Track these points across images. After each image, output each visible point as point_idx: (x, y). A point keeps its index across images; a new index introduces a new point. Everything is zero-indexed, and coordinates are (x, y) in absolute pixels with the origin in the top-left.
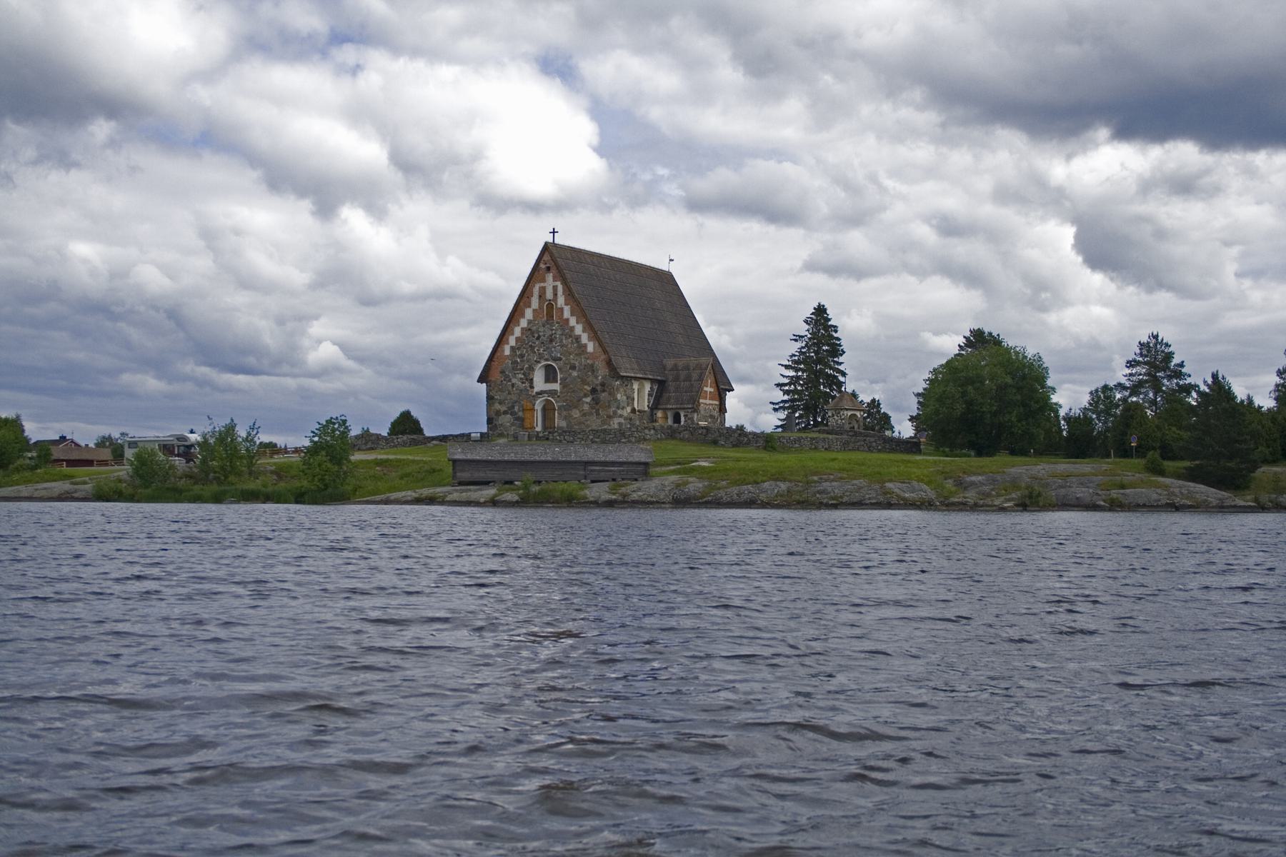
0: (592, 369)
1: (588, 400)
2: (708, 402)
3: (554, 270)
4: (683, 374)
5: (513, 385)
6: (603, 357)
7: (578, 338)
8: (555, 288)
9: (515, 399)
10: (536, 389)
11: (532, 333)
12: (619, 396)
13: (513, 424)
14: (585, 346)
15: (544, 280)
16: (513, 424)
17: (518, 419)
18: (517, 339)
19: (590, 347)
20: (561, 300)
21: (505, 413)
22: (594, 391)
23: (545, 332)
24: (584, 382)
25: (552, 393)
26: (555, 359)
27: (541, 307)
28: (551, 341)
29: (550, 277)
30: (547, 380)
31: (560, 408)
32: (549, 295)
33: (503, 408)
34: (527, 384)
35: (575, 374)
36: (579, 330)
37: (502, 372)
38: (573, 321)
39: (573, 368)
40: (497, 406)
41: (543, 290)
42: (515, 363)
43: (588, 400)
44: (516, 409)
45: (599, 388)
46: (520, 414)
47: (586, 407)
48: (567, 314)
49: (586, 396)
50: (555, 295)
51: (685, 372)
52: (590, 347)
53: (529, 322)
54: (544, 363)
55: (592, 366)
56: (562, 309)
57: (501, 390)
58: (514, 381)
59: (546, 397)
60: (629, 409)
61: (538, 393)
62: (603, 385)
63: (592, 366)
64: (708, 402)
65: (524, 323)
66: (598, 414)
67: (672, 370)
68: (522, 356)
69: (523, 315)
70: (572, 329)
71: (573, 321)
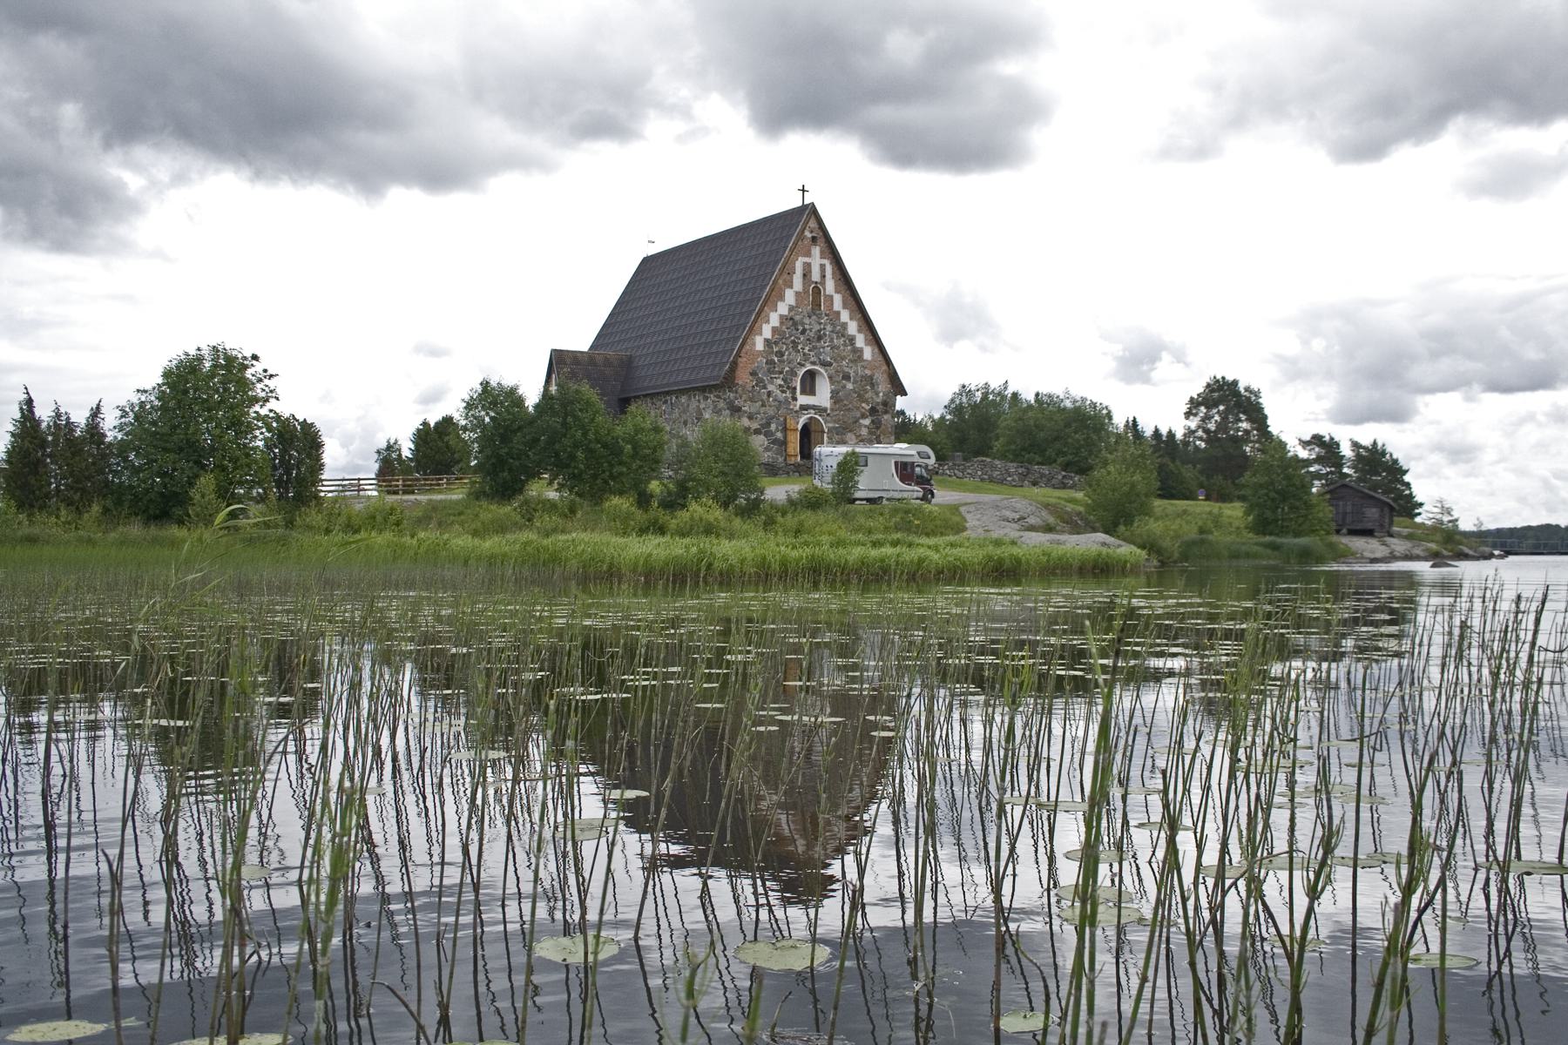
0: (870, 381)
1: (867, 422)
3: (821, 241)
5: (769, 394)
6: (885, 367)
7: (852, 340)
8: (823, 267)
9: (771, 412)
11: (795, 324)
13: (767, 449)
14: (861, 350)
15: (808, 254)
16: (767, 449)
17: (775, 442)
18: (774, 330)
19: (868, 353)
20: (830, 286)
21: (757, 432)
22: (873, 411)
23: (812, 325)
24: (861, 398)
25: (820, 410)
26: (825, 364)
27: (805, 291)
28: (820, 338)
29: (816, 251)
30: (803, 392)
31: (830, 430)
32: (816, 276)
33: (755, 426)
34: (788, 394)
35: (850, 386)
36: (853, 328)
37: (754, 374)
38: (845, 316)
39: (847, 377)
40: (746, 422)
41: (807, 267)
42: (770, 362)
43: (867, 422)
44: (773, 427)
45: (880, 408)
46: (779, 435)
47: (864, 432)
48: (838, 301)
49: (863, 416)
50: (824, 276)
52: (868, 353)
53: (791, 308)
54: (809, 367)
55: (871, 377)
57: (752, 400)
58: (771, 388)
59: (812, 414)
62: (885, 404)
63: (871, 377)
65: (783, 309)
69: (782, 298)
70: (844, 326)
71: (845, 316)
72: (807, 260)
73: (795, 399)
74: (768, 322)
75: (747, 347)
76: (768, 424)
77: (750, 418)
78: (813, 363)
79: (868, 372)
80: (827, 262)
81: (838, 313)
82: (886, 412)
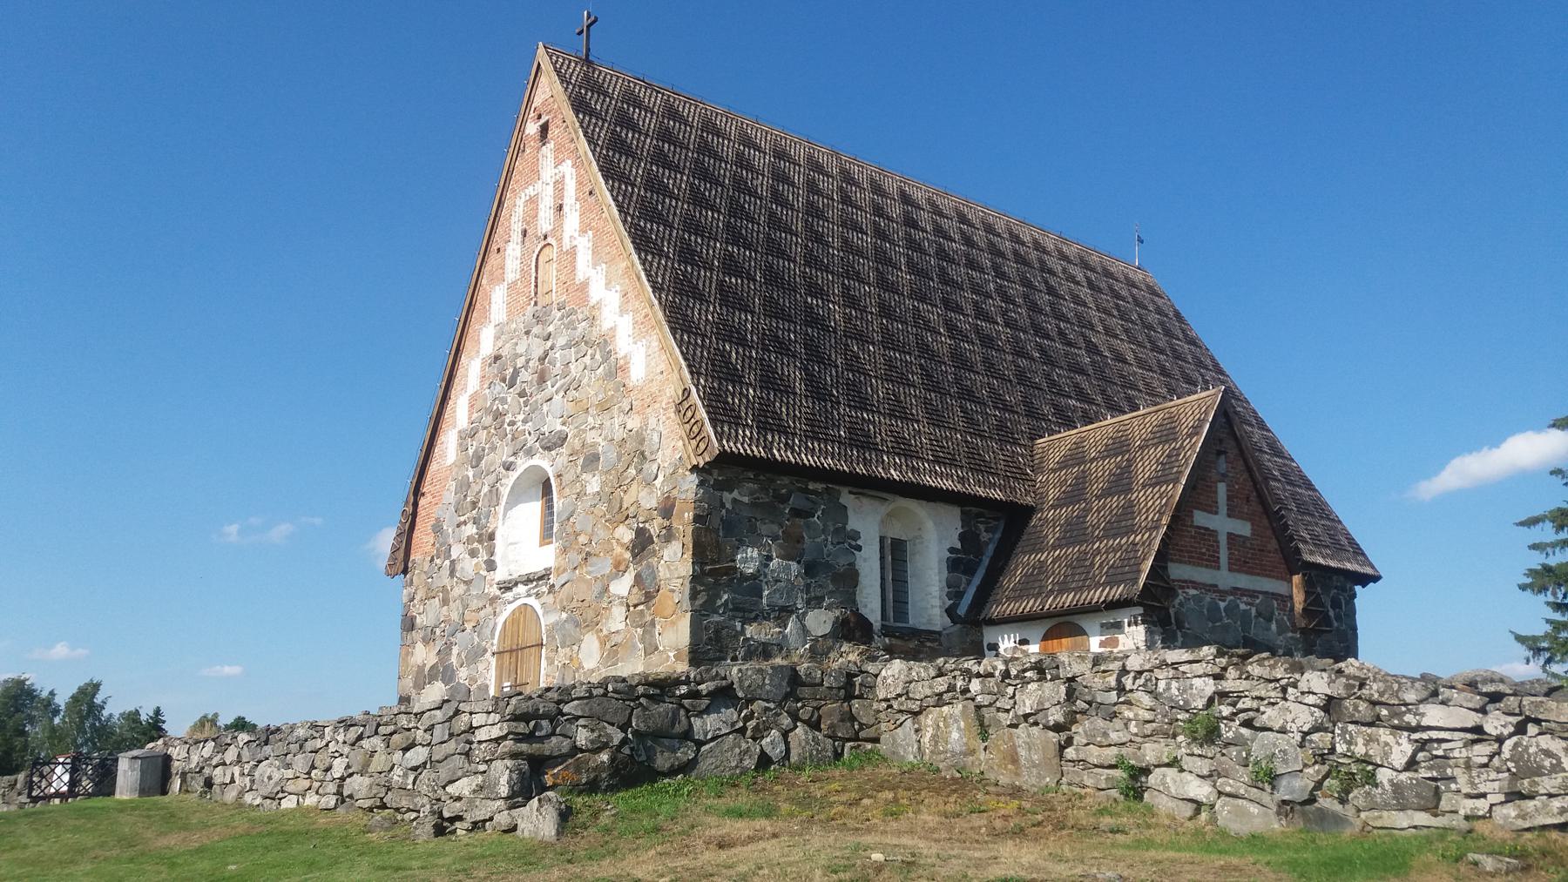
0: (638, 452)
1: (622, 586)
2: (1225, 578)
4: (1101, 471)
7: (604, 345)
10: (500, 575)
12: (748, 559)
15: (535, 173)
22: (642, 544)
28: (542, 380)
32: (545, 223)
35: (593, 484)
39: (592, 460)
42: (464, 485)
45: (654, 528)
47: (616, 620)
49: (619, 569)
51: (1110, 464)
56: (573, 252)
60: (820, 621)
61: (506, 587)
62: (667, 510)
64: (1225, 578)
66: (650, 649)
67: (1063, 465)
68: (479, 457)
72: (530, 191)
73: (491, 566)
74: (464, 389)
75: (433, 467)
76: (449, 647)
77: (426, 641)
78: (530, 453)
79: (634, 423)
80: (567, 168)
81: (584, 286)
82: (669, 536)
